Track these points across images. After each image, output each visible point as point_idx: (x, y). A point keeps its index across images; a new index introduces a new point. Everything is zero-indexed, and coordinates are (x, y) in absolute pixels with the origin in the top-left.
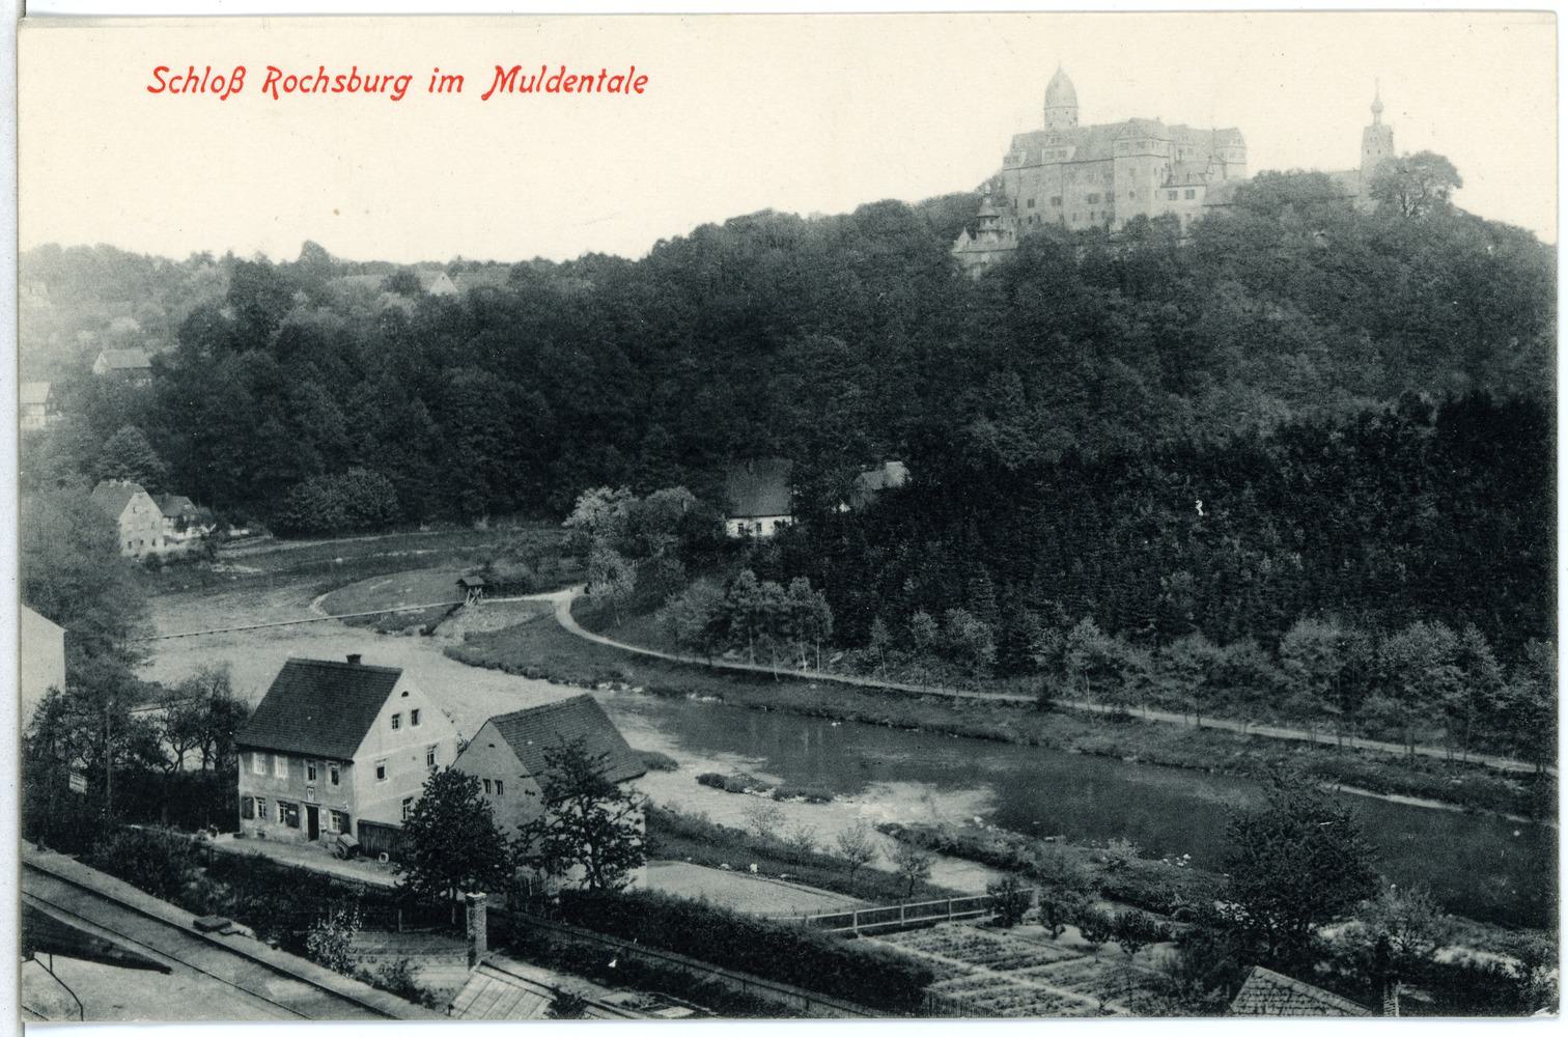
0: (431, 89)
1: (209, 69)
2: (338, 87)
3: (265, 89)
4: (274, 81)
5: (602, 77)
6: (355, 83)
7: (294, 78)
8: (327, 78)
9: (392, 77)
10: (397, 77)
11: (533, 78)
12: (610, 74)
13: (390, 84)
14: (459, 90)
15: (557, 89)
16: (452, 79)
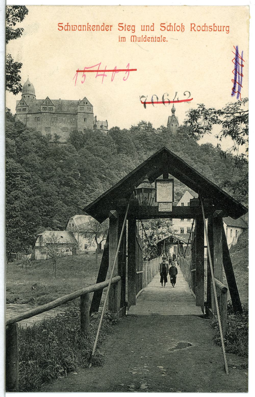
0: (119, 41)
1: (175, 24)
2: (211, 30)
3: (191, 30)
4: (193, 28)
5: (156, 38)
6: (215, 28)
7: (200, 26)
8: (207, 26)
9: (225, 27)
10: (226, 27)
11: (140, 38)
12: (157, 37)
13: (225, 28)
14: (125, 41)
15: (146, 41)
16: (123, 38)
